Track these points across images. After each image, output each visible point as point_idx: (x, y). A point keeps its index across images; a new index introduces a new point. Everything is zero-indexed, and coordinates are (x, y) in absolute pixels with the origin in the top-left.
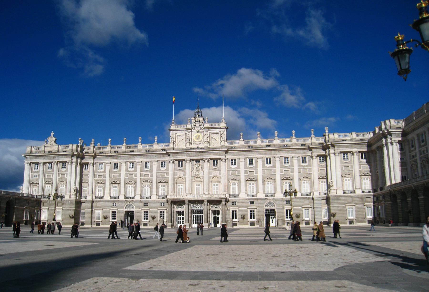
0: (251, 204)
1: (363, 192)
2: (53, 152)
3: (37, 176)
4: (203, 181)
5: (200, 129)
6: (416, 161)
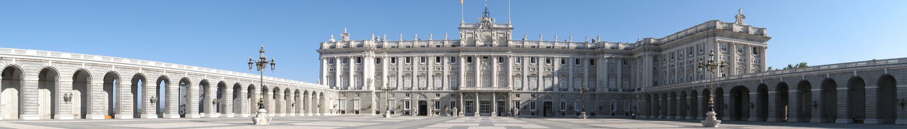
1: (623, 91)
6: (666, 72)
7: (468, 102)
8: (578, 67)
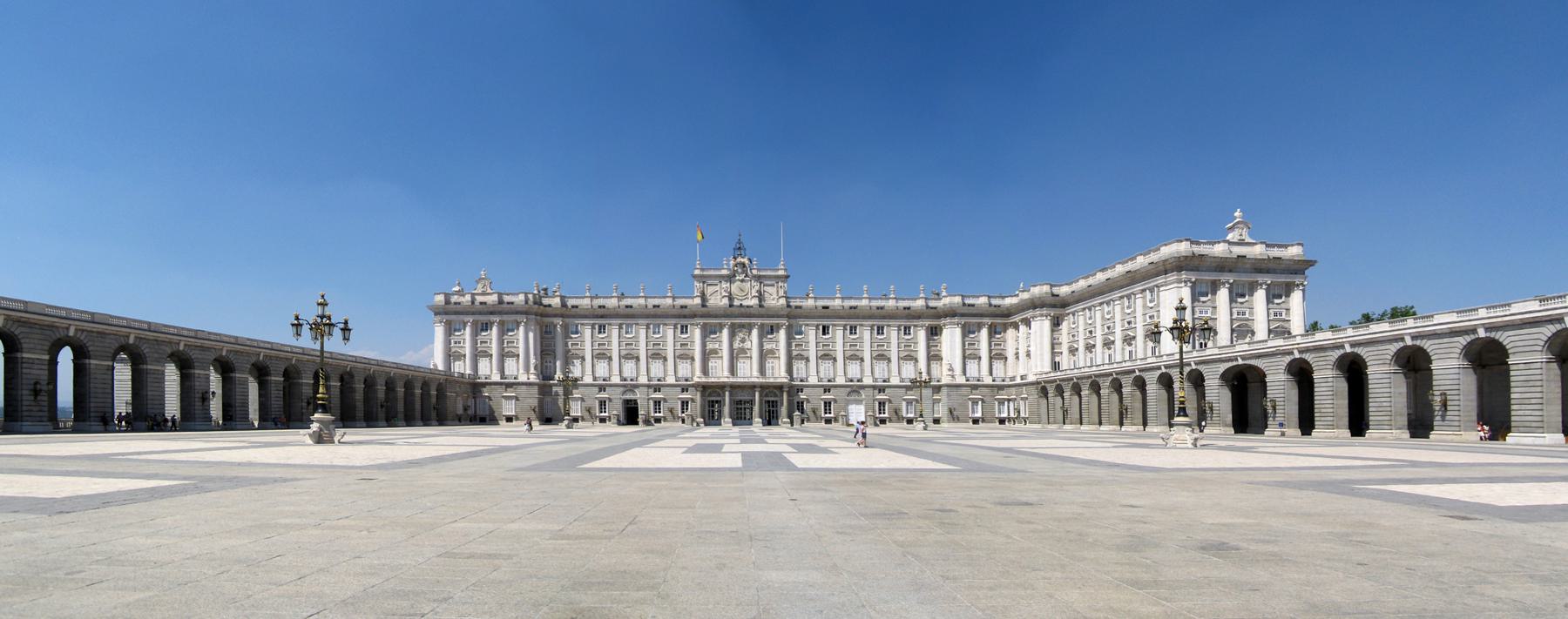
0: (825, 392)
1: (994, 381)
7: (713, 401)
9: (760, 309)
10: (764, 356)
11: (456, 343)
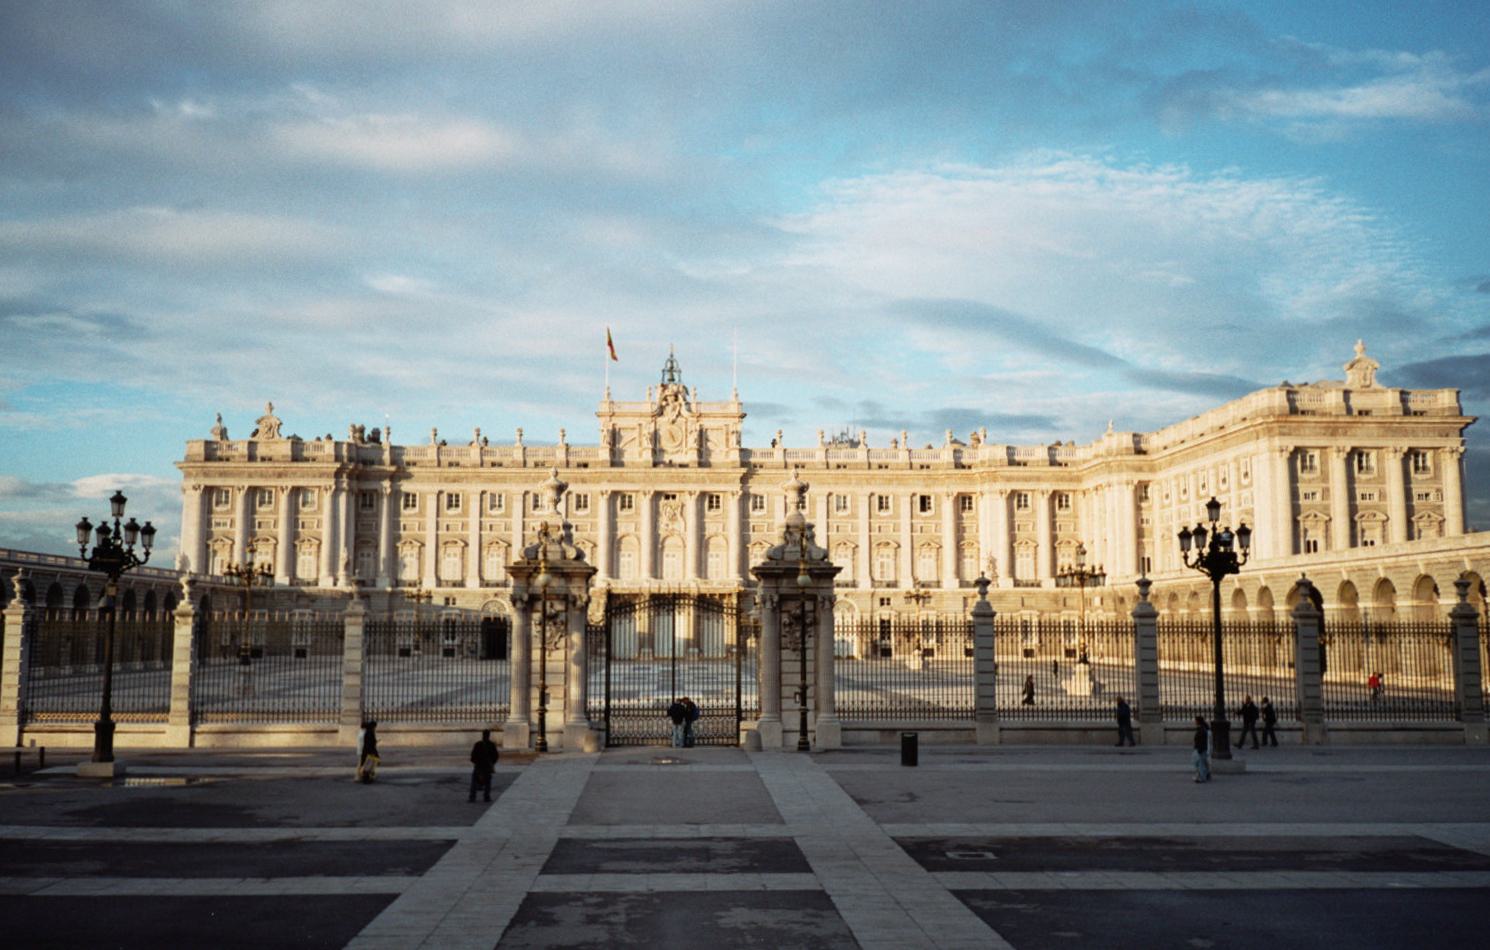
2: (275, 458)
3: (225, 524)
4: (685, 547)
5: (677, 416)
8: (923, 518)
9: (700, 470)
10: (703, 544)
11: (218, 524)
